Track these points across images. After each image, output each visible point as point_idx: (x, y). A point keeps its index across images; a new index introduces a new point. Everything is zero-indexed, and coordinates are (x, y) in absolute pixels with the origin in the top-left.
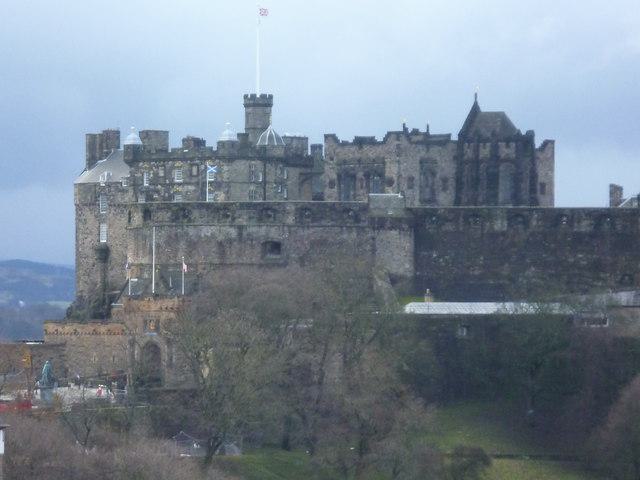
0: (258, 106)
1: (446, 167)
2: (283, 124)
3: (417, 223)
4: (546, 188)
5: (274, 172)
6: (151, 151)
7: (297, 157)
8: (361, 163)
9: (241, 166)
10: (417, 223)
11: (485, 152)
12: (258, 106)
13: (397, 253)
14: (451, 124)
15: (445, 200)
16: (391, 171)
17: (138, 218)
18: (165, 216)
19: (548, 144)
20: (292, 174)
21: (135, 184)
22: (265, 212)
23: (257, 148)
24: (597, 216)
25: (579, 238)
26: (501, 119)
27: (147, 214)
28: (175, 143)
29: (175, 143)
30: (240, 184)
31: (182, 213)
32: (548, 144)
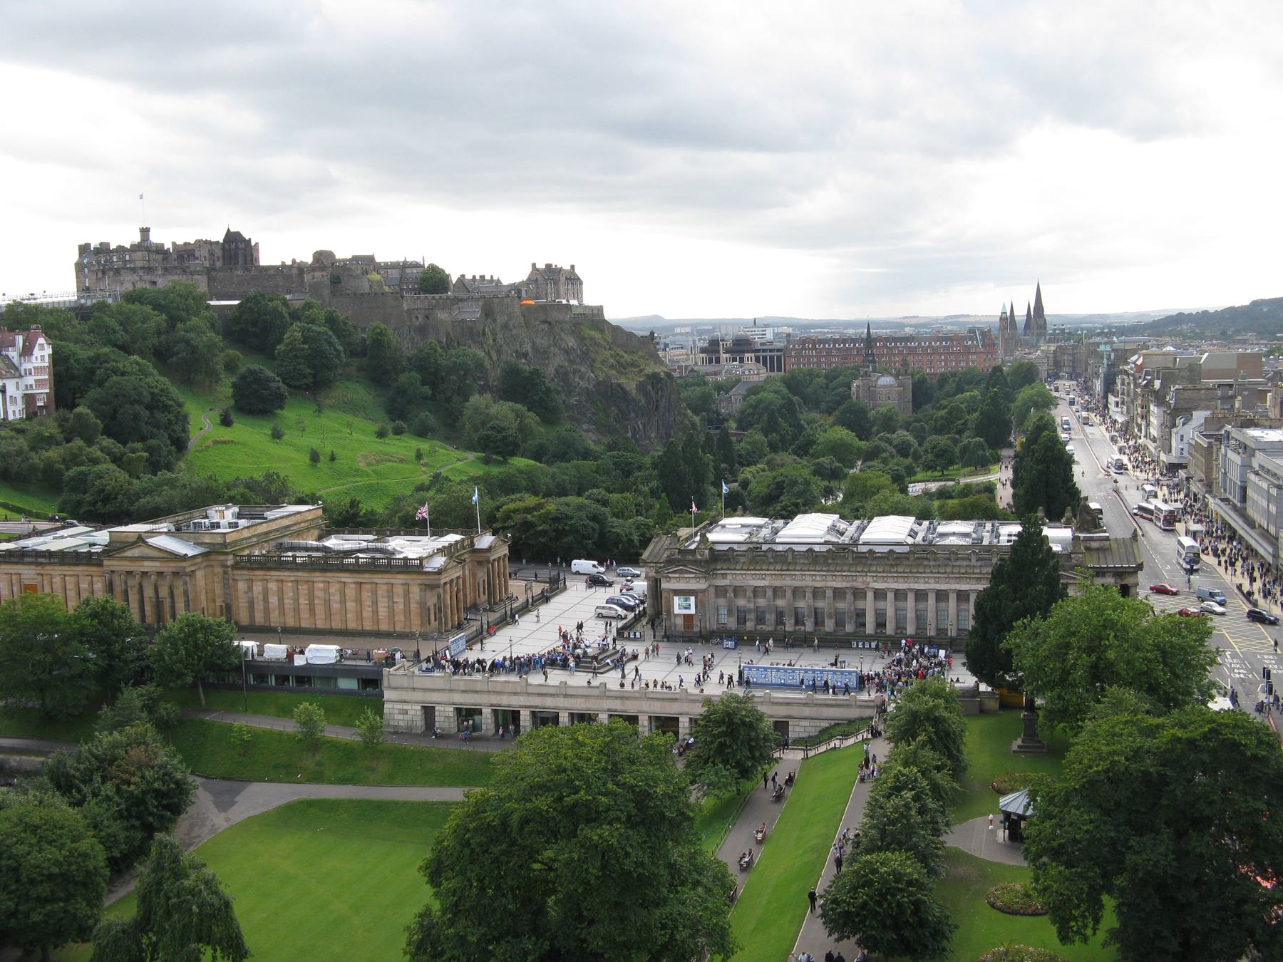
0: (145, 232)
1: (218, 252)
2: (155, 238)
3: (209, 271)
4: (257, 260)
5: (153, 256)
6: (103, 249)
7: (159, 249)
8: (185, 253)
9: (139, 254)
10: (209, 271)
11: (233, 246)
12: (145, 232)
13: (202, 285)
14: (219, 237)
15: (219, 264)
16: (197, 254)
17: (100, 275)
18: (111, 273)
19: (257, 244)
20: (160, 257)
21: (99, 263)
22: (150, 270)
23: (145, 246)
24: (276, 268)
25: (270, 276)
26: (238, 234)
27: (104, 273)
28: (113, 247)
29: (113, 247)
30: (140, 259)
31: (117, 272)
32: (257, 244)
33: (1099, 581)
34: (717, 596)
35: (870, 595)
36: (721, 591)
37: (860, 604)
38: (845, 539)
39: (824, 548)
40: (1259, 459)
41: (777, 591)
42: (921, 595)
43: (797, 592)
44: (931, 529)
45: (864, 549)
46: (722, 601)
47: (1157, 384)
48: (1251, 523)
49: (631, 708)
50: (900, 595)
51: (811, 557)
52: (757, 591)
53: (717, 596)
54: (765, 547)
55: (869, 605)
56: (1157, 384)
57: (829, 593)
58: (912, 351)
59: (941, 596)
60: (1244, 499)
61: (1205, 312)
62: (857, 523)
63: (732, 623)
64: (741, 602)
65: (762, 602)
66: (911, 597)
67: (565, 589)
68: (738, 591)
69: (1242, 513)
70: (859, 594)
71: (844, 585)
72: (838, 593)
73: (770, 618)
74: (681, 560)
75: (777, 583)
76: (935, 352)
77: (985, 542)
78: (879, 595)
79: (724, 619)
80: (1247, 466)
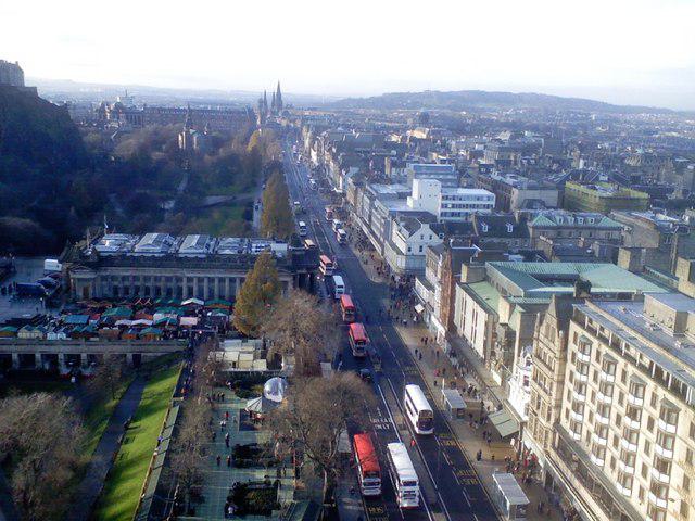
33: (299, 272)
34: (102, 280)
35: (185, 279)
36: (104, 278)
37: (179, 284)
38: (172, 250)
39: (161, 255)
40: (377, 203)
41: (135, 278)
42: (211, 280)
43: (146, 279)
44: (217, 243)
45: (180, 256)
46: (104, 283)
47: (334, 150)
48: (373, 233)
49: (52, 350)
50: (200, 280)
51: (155, 262)
52: (124, 278)
53: (102, 280)
54: (128, 255)
55: (184, 284)
56: (334, 150)
57: (163, 279)
58: (213, 118)
59: (222, 280)
60: (370, 220)
61: (361, 99)
62: (179, 238)
63: (111, 295)
64: (116, 283)
65: (127, 283)
66: (206, 280)
67: (15, 272)
68: (113, 278)
69: (369, 226)
70: (179, 279)
71: (171, 275)
72: (168, 279)
73: (132, 292)
74: (84, 262)
75: (137, 274)
76: (224, 118)
77: (244, 252)
78: (190, 280)
79: (106, 293)
80: (372, 205)
